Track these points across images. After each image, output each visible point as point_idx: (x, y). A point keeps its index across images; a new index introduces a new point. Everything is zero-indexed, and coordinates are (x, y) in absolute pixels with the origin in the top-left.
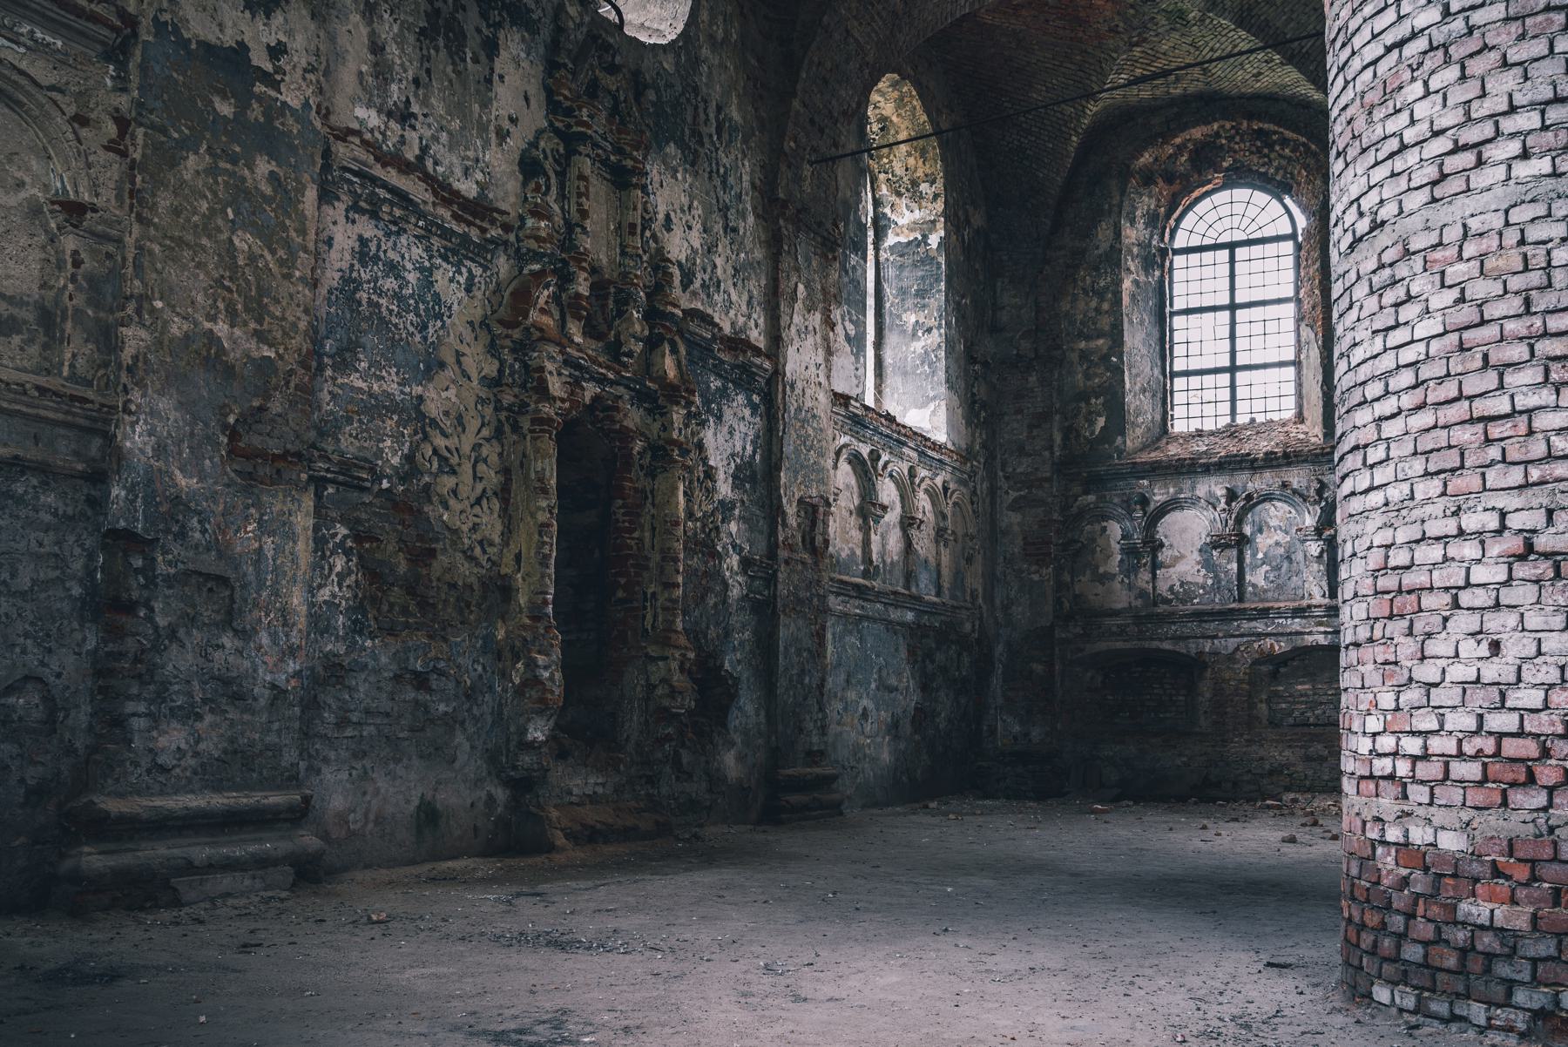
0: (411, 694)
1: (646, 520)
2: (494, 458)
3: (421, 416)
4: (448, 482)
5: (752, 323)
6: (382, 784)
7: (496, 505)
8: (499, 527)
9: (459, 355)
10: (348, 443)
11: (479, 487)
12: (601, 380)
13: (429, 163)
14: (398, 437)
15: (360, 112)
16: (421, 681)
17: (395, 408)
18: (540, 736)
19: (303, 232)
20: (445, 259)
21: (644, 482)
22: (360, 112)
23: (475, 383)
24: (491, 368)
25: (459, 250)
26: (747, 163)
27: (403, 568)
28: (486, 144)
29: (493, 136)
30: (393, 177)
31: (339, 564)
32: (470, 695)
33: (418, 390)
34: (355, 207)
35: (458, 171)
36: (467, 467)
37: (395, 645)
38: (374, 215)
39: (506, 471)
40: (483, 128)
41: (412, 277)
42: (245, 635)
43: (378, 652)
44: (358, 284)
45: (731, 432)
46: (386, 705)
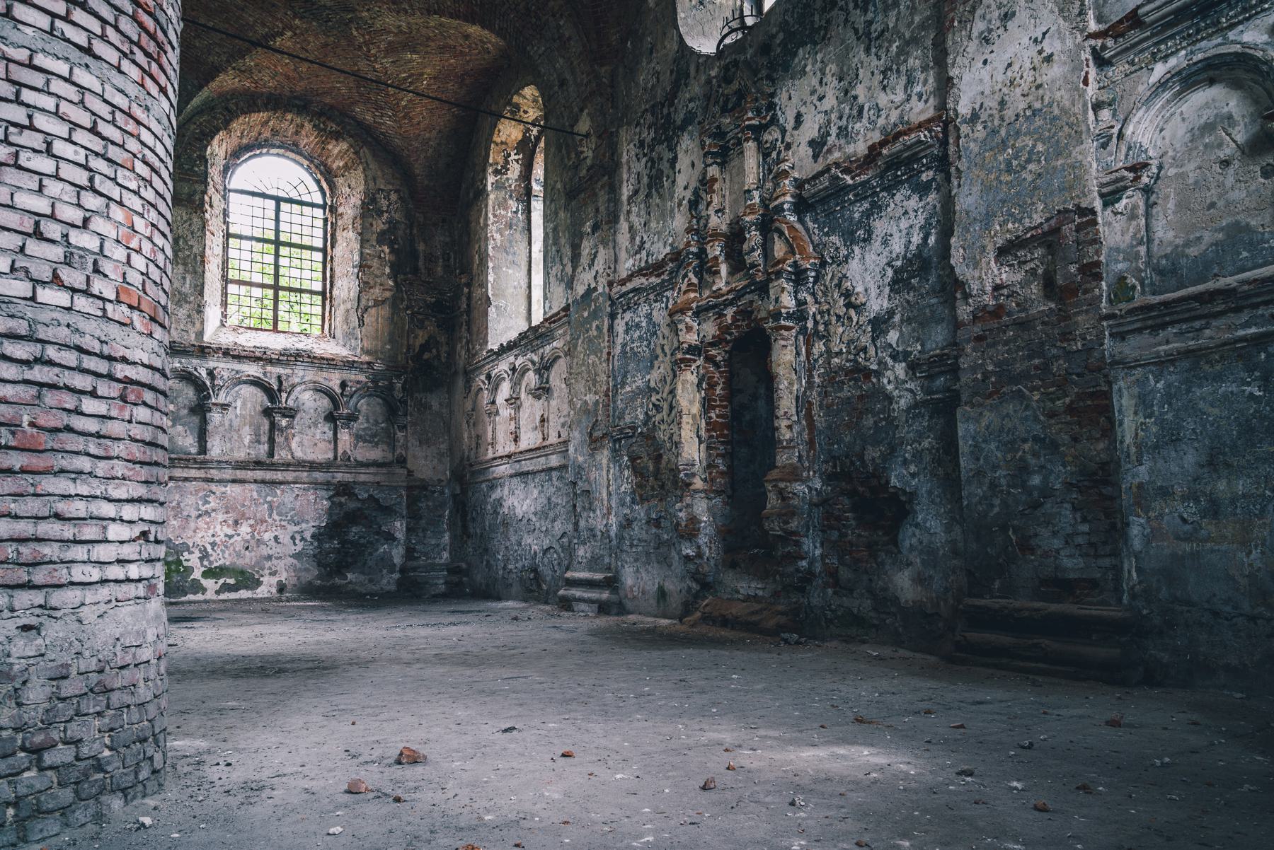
42: (594, 511)
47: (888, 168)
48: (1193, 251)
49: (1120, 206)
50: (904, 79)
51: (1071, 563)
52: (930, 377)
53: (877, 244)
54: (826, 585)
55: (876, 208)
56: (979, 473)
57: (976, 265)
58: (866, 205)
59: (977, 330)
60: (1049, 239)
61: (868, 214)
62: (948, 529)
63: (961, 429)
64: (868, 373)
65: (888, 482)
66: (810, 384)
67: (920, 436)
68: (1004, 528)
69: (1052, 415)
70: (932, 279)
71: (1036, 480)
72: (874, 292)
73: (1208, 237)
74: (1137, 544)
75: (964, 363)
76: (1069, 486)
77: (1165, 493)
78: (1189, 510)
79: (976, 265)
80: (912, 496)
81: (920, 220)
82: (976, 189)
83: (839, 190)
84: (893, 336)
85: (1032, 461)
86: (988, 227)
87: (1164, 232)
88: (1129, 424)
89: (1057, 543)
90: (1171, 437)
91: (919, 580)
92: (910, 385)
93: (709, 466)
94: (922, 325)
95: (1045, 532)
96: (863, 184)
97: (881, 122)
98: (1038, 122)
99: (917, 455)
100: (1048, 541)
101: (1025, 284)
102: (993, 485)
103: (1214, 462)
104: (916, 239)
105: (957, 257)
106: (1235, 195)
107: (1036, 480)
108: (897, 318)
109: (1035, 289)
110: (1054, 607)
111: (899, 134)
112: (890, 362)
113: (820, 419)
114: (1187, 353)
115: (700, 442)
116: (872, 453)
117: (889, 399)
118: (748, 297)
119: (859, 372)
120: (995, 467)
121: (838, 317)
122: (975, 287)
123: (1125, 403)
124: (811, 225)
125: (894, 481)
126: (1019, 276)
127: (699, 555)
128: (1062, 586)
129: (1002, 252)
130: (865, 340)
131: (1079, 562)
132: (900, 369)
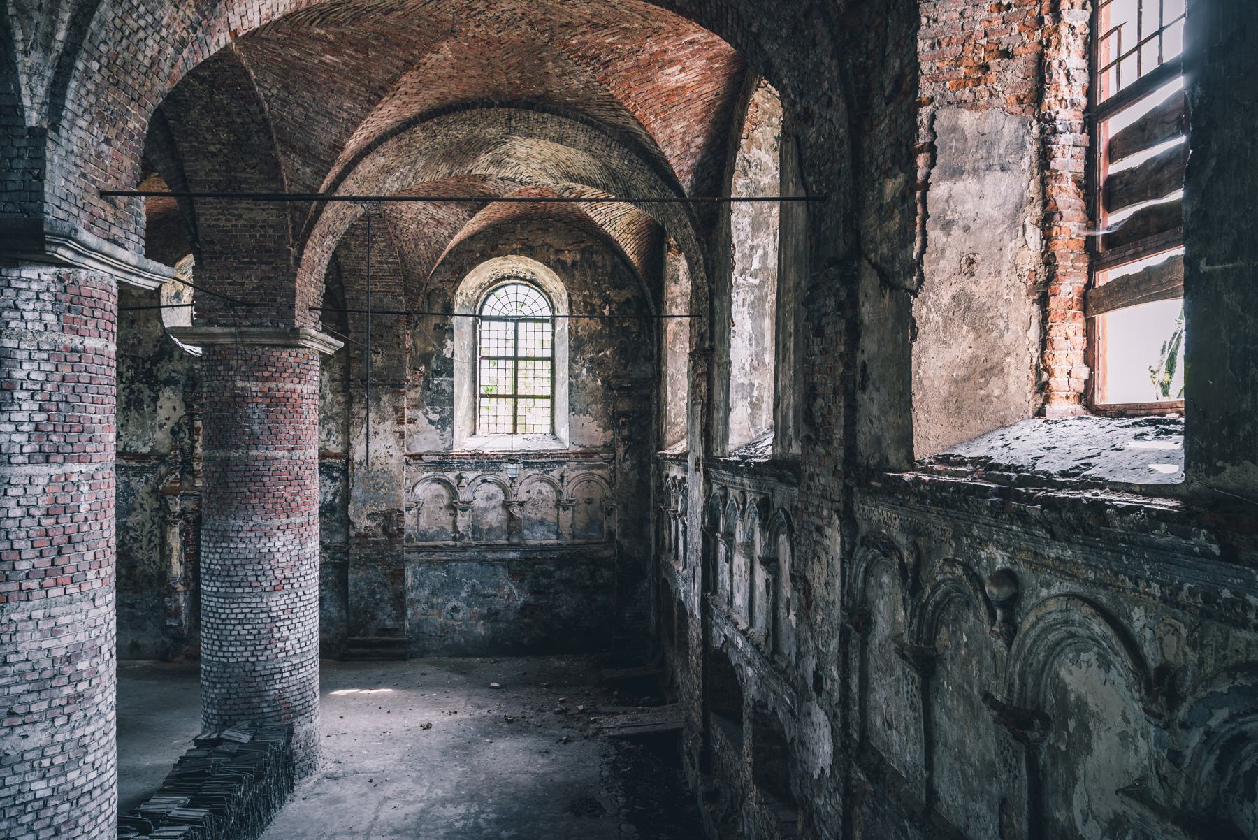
4: (136, 546)
5: (331, 442)
9: (142, 505)
11: (152, 545)
13: (128, 449)
16: (131, 606)
18: (173, 624)
20: (135, 476)
24: (156, 505)
28: (154, 432)
29: (157, 429)
32: (153, 609)
33: (124, 520)
35: (141, 446)
36: (145, 541)
40: (152, 428)
48: (431, 531)
49: (411, 512)
50: (326, 432)
51: (389, 623)
52: (334, 554)
56: (356, 593)
57: (359, 518)
59: (357, 541)
60: (387, 516)
62: (339, 611)
63: (350, 576)
68: (365, 612)
69: (385, 575)
71: (378, 596)
73: (435, 528)
74: (409, 616)
75: (351, 552)
76: (390, 599)
77: (419, 601)
78: (425, 607)
79: (359, 518)
81: (332, 491)
82: (361, 490)
85: (377, 590)
86: (364, 505)
87: (423, 523)
88: (410, 580)
89: (385, 617)
90: (422, 585)
94: (331, 532)
95: (380, 613)
98: (386, 475)
100: (381, 616)
101: (375, 527)
102: (362, 597)
103: (432, 594)
104: (329, 498)
105: (351, 512)
106: (443, 519)
107: (378, 596)
109: (380, 530)
110: (384, 638)
114: (428, 561)
115: (181, 564)
120: (363, 591)
122: (358, 525)
123: (409, 573)
126: (374, 524)
127: (180, 625)
128: (385, 631)
129: (370, 516)
131: (392, 623)
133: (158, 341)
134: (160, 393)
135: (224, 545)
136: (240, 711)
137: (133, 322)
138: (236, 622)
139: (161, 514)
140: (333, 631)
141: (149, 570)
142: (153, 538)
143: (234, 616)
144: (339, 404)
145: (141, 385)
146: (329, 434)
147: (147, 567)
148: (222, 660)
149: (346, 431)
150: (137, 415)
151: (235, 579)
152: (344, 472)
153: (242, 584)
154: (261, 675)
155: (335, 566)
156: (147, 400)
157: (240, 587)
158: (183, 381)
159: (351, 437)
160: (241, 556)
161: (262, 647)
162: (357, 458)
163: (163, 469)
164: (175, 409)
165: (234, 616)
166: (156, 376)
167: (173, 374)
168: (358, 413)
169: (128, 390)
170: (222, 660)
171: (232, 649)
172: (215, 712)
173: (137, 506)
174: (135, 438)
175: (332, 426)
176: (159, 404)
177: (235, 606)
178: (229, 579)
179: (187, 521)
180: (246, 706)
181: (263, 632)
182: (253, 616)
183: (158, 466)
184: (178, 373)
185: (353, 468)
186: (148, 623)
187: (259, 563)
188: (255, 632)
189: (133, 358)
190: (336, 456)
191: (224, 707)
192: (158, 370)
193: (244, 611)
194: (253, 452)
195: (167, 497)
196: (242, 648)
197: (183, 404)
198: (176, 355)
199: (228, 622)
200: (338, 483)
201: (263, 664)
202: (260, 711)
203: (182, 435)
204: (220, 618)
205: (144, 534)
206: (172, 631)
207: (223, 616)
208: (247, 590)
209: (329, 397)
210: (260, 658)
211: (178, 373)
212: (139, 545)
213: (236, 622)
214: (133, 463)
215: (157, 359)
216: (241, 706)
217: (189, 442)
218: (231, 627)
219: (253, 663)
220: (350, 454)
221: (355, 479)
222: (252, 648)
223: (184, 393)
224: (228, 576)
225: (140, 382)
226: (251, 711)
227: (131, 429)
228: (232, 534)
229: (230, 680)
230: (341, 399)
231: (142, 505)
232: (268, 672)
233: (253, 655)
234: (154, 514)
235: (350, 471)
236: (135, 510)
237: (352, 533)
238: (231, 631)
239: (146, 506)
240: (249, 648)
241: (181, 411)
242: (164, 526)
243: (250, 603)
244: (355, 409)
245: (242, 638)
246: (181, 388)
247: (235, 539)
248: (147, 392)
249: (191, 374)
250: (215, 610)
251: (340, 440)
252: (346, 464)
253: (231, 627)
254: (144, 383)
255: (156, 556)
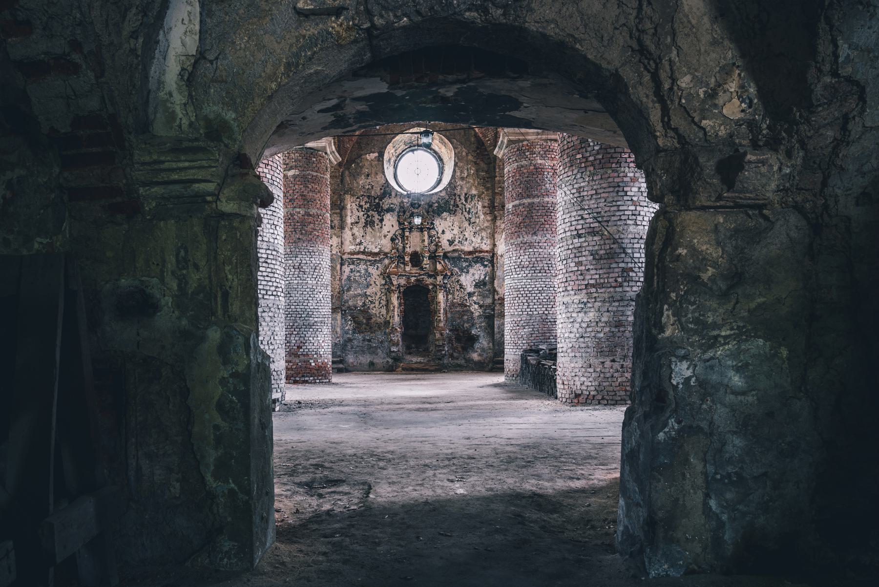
0: (367, 343)
1: (435, 303)
2: (385, 299)
3: (366, 295)
4: (372, 306)
5: (483, 244)
6: (361, 358)
7: (385, 307)
8: (385, 312)
9: (375, 282)
10: (350, 303)
11: (381, 305)
12: (415, 276)
13: (366, 250)
14: (361, 300)
15: (350, 247)
16: (369, 341)
17: (360, 295)
18: (395, 350)
19: (337, 273)
20: (371, 265)
21: (434, 294)
22: (350, 247)
23: (379, 286)
24: (383, 282)
25: (373, 263)
26: (480, 203)
27: (364, 321)
29: (383, 238)
30: (355, 256)
31: (350, 323)
33: (365, 291)
34: (349, 264)
35: (374, 248)
36: (377, 303)
37: (362, 335)
38: (353, 264)
39: (387, 301)
40: (380, 237)
41: (363, 272)
43: (360, 337)
44: (351, 277)
45: (473, 275)
46: (361, 344)
47: (476, 257)
50: (480, 238)
52: (485, 310)
53: (470, 274)
54: (449, 357)
55: (470, 265)
58: (467, 264)
59: (500, 302)
61: (468, 266)
62: (488, 344)
63: (496, 322)
64: (466, 306)
65: (471, 333)
66: (447, 305)
67: (481, 323)
70: (487, 287)
72: (469, 286)
75: (496, 308)
80: (478, 336)
81: (484, 273)
83: (459, 258)
84: (475, 298)
91: (480, 355)
92: (479, 310)
93: (400, 324)
94: (483, 297)
96: (467, 258)
97: (473, 245)
99: (480, 327)
104: (483, 277)
108: (476, 294)
111: (476, 252)
112: (473, 304)
113: (449, 315)
115: (398, 316)
116: (466, 325)
117: (473, 313)
118: (423, 277)
119: (463, 305)
121: (457, 290)
122: (500, 293)
124: (447, 263)
125: (473, 332)
130: (467, 298)
132: (476, 306)
133: (383, 186)
134: (384, 217)
135: (530, 250)
136: (540, 340)
137: (368, 175)
138: (538, 292)
139: (387, 287)
140: (485, 355)
141: (379, 320)
142: (382, 301)
143: (536, 289)
144: (488, 221)
145: (373, 213)
146: (482, 239)
147: (378, 318)
148: (529, 313)
149: (492, 236)
150: (371, 230)
151: (538, 268)
152: (492, 262)
153: (542, 271)
154: (550, 322)
155: (486, 317)
156: (377, 221)
157: (540, 272)
158: (397, 210)
159: (496, 240)
160: (540, 256)
161: (551, 306)
162: (499, 253)
163: (387, 261)
164: (393, 226)
165: (536, 289)
166: (382, 207)
167: (392, 206)
168: (500, 226)
169: (366, 216)
170: (529, 313)
171: (536, 307)
172: (524, 342)
173: (372, 283)
174: (370, 243)
175: (484, 234)
176: (384, 223)
177: (538, 283)
178: (534, 269)
179: (400, 292)
180: (543, 337)
181: (552, 298)
182: (546, 289)
183: (384, 258)
184: (394, 205)
185: (497, 259)
186: (379, 350)
187: (550, 260)
188: (547, 297)
189: (369, 197)
190: (487, 252)
191: (531, 339)
192: (383, 203)
193: (542, 286)
194: (546, 199)
195: (391, 276)
196: (542, 306)
197: (397, 223)
198: (393, 194)
199: (533, 292)
200: (487, 268)
201: (551, 315)
202: (550, 341)
203: (397, 241)
204: (528, 290)
205: (377, 299)
206: (393, 354)
207: (530, 289)
208: (544, 274)
209: (482, 217)
210: (550, 312)
211: (394, 205)
212: (374, 305)
213: (538, 292)
214: (370, 258)
215: (382, 197)
216: (541, 338)
217: (402, 245)
218: (535, 295)
219: (546, 315)
220: (495, 250)
221: (498, 265)
222: (546, 306)
223: (399, 216)
224: (533, 267)
225: (373, 210)
226: (545, 340)
227: (368, 238)
228: (535, 244)
229: (534, 324)
230: (489, 218)
231: (375, 282)
232: (553, 320)
233: (546, 310)
234: (382, 287)
235: (495, 260)
236: (371, 285)
237: (496, 297)
238: (534, 297)
239: (377, 283)
240: (545, 306)
241: (396, 227)
242: (388, 294)
243: (545, 282)
244: (498, 223)
245: (541, 301)
246: (396, 214)
247: (537, 247)
248: (377, 217)
249: (402, 205)
250: (524, 286)
251: (488, 242)
252: (493, 257)
253: (535, 295)
254: (375, 211)
255: (384, 311)
